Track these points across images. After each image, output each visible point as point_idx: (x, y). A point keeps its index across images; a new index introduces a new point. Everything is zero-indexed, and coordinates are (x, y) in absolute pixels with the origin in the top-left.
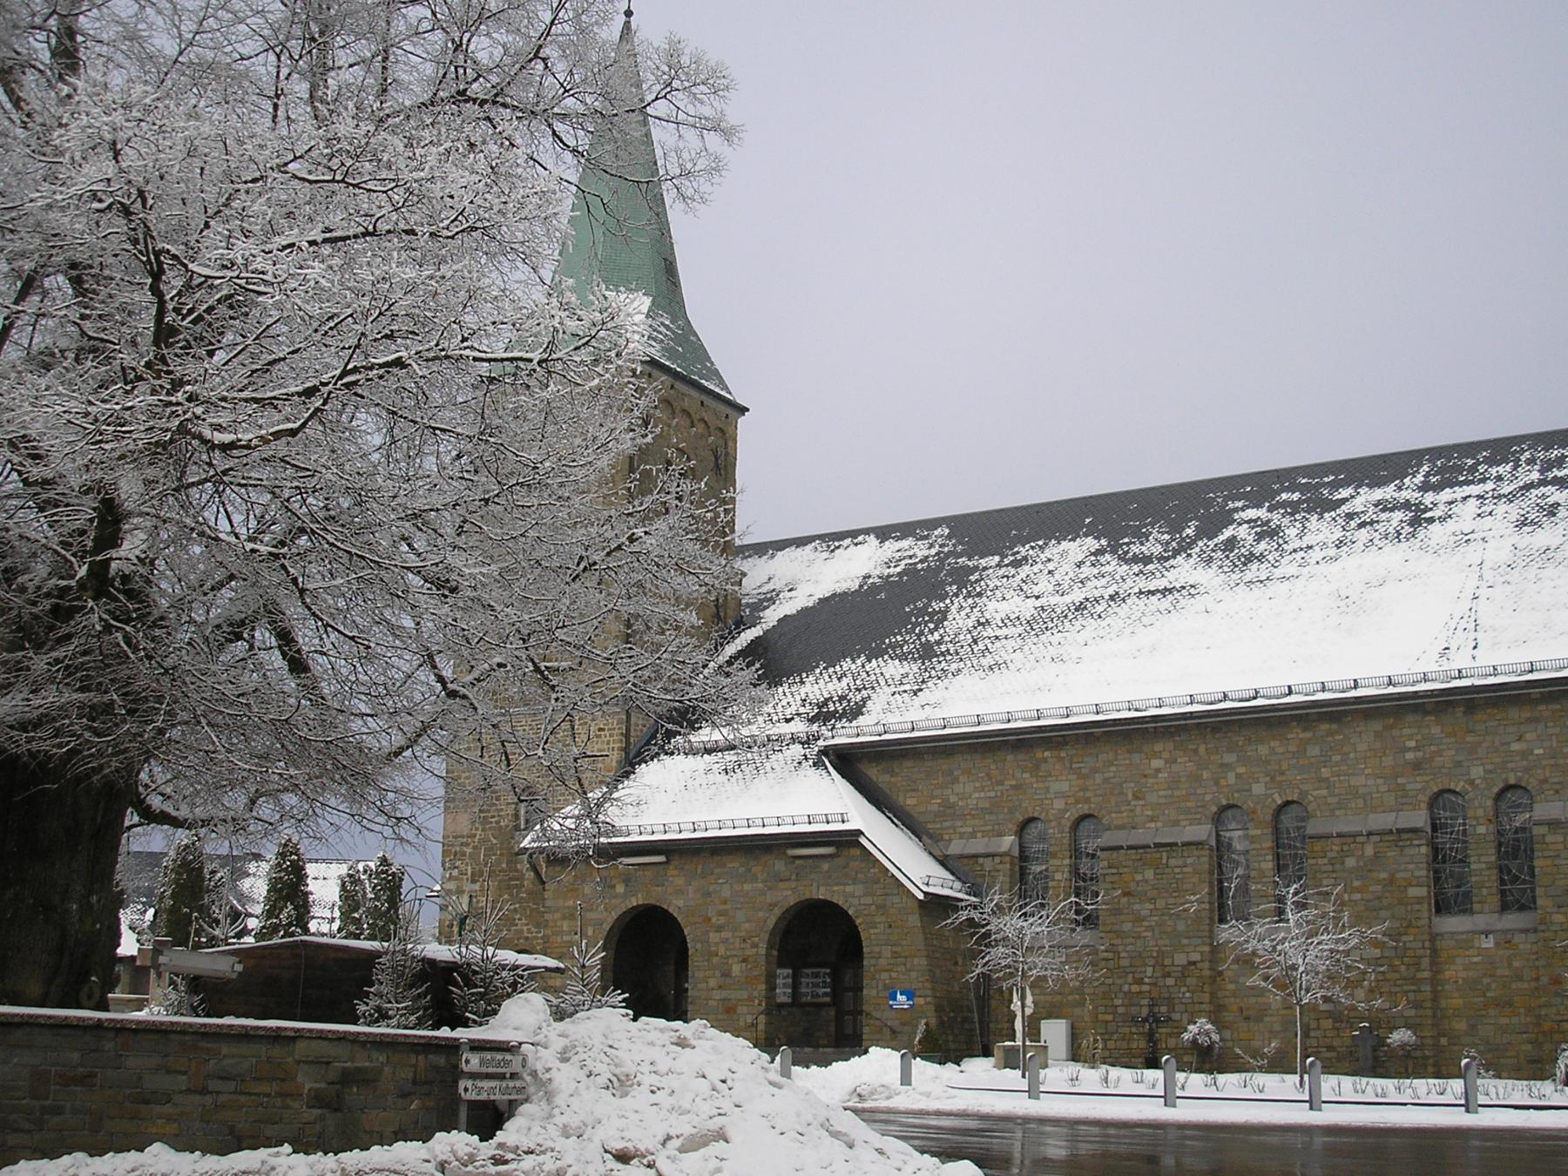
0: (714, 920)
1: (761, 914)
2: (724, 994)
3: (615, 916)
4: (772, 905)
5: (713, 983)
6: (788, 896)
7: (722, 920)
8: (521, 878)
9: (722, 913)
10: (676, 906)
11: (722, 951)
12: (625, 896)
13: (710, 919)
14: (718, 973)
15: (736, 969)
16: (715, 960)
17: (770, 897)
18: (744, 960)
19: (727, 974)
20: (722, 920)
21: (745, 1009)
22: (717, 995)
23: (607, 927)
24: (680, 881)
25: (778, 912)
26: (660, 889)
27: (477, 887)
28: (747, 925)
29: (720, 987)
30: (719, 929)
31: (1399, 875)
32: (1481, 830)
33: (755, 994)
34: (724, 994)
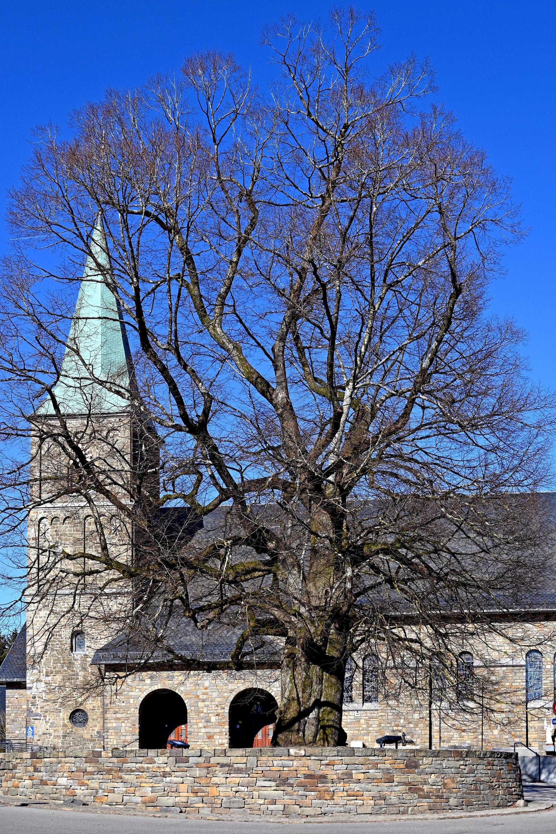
0: (201, 697)
1: (226, 694)
2: (207, 730)
3: (145, 694)
4: (232, 691)
5: (201, 725)
6: (240, 686)
7: (205, 697)
8: (77, 675)
9: (204, 694)
10: (180, 691)
11: (205, 711)
12: (151, 685)
13: (198, 696)
14: (203, 721)
15: (213, 719)
16: (202, 715)
17: (231, 687)
18: (218, 715)
19: (208, 721)
20: (205, 697)
21: (218, 737)
22: (203, 730)
23: (141, 699)
24: (182, 678)
25: (235, 693)
26: (170, 682)
27: (50, 678)
28: (219, 699)
29: (205, 727)
30: (204, 701)
31: (514, 684)
32: (548, 667)
33: (224, 730)
34: (207, 730)
